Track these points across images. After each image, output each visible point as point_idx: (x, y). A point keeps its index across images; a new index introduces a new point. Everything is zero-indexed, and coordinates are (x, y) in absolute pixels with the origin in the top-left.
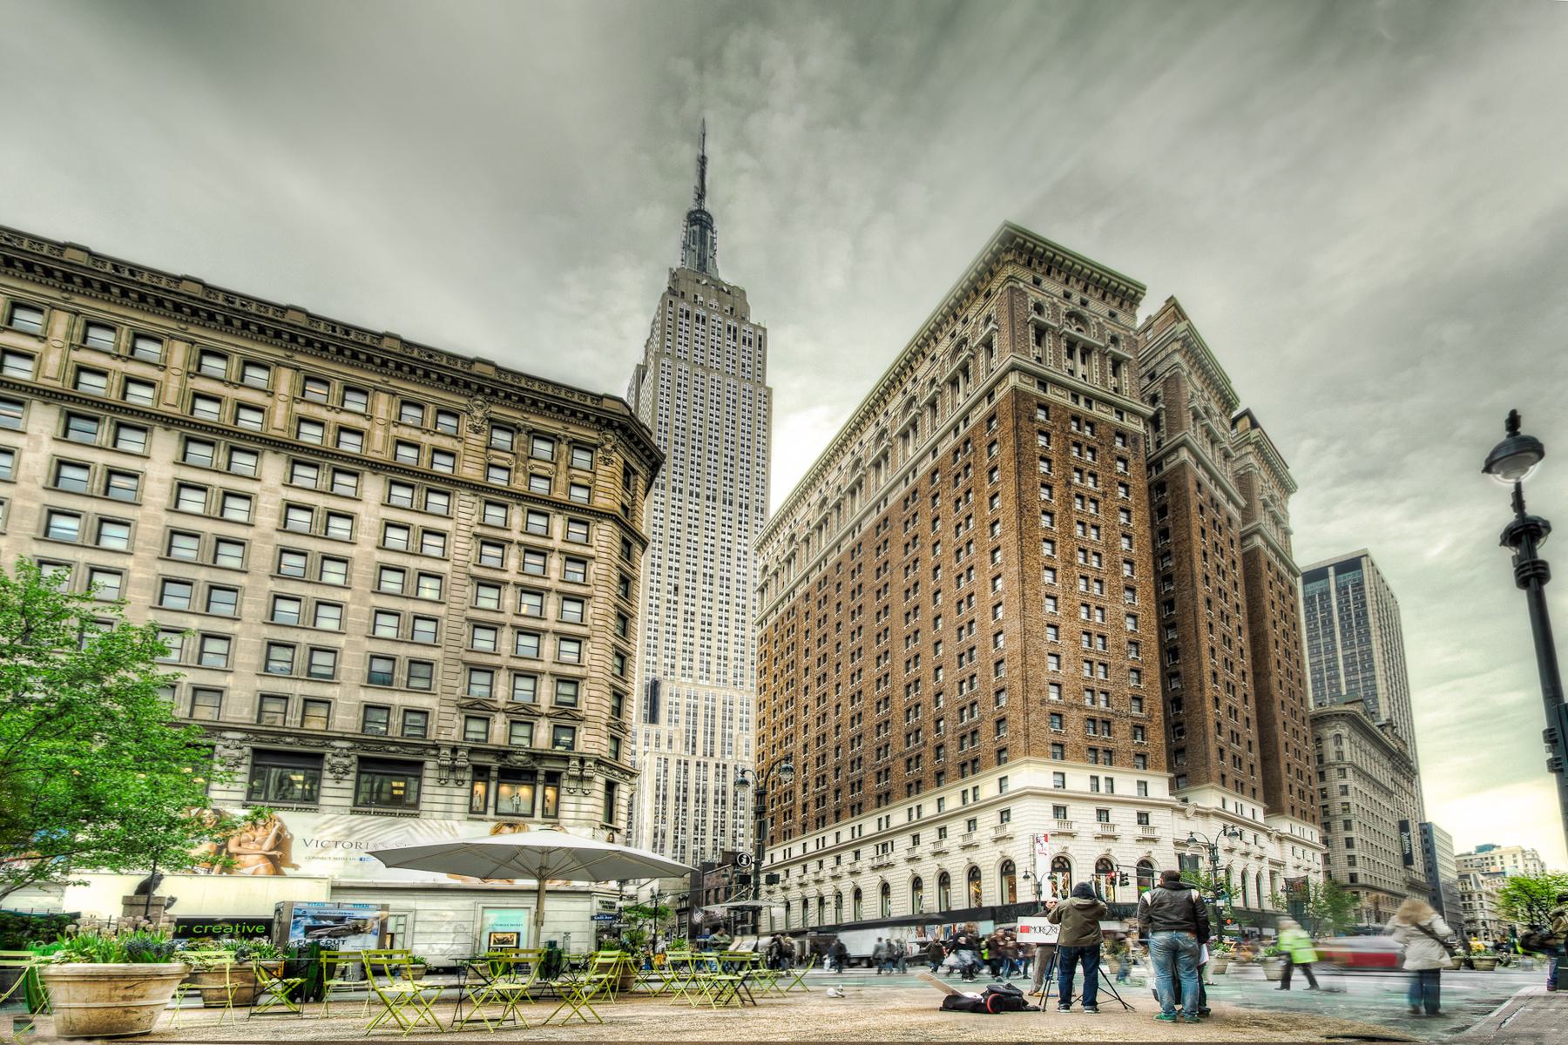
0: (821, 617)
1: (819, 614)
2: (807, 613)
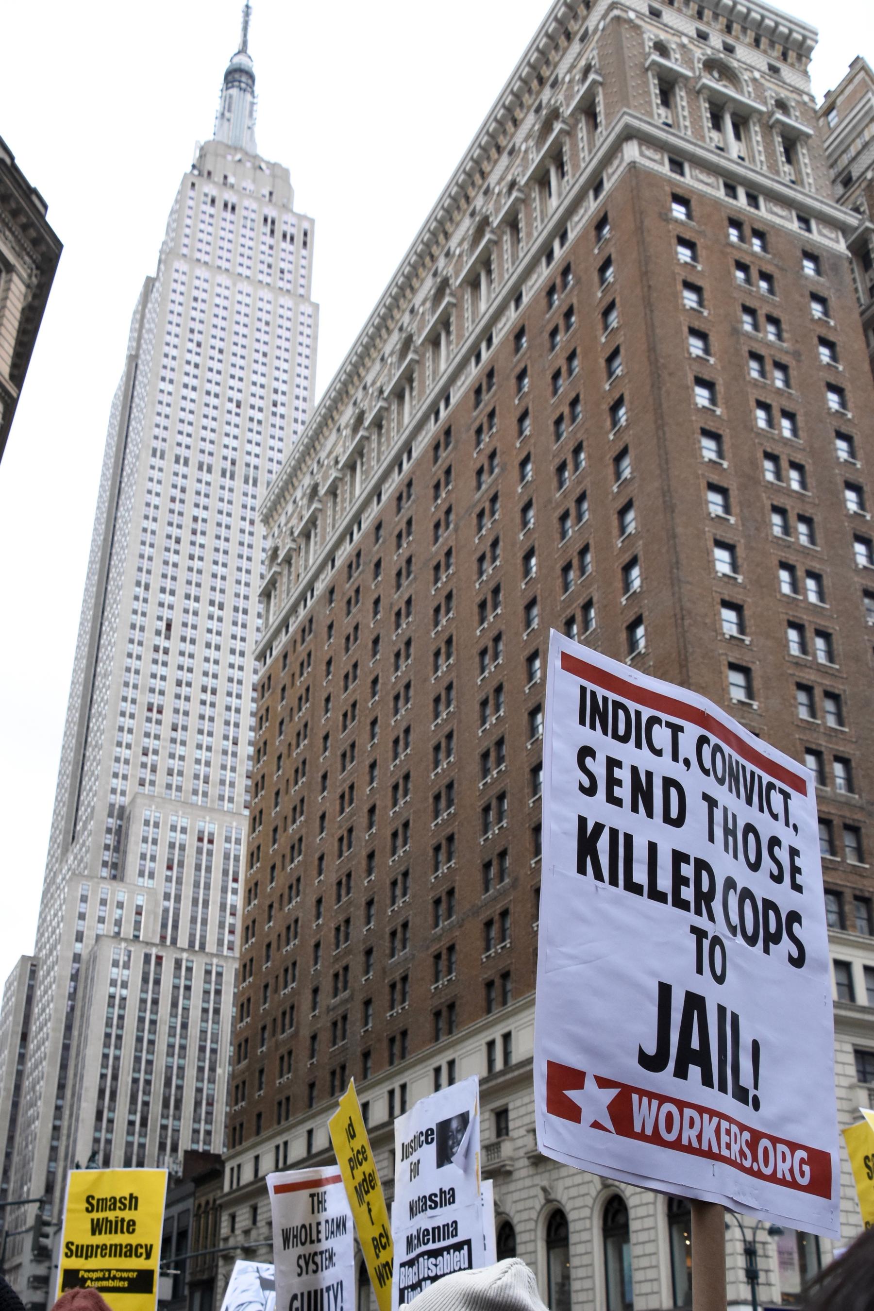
0: (351, 630)
1: (345, 625)
2: (331, 627)
